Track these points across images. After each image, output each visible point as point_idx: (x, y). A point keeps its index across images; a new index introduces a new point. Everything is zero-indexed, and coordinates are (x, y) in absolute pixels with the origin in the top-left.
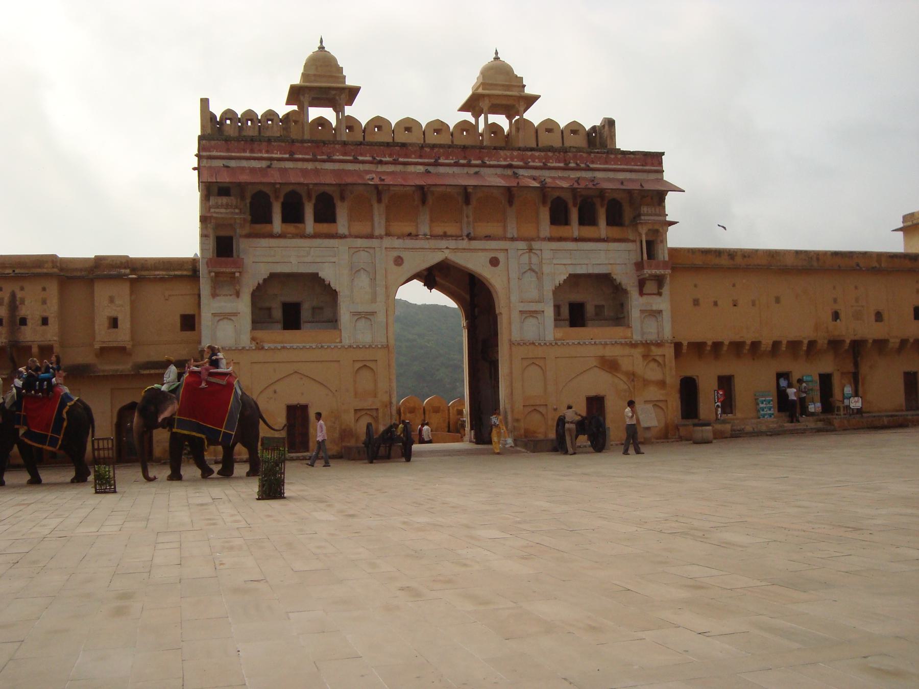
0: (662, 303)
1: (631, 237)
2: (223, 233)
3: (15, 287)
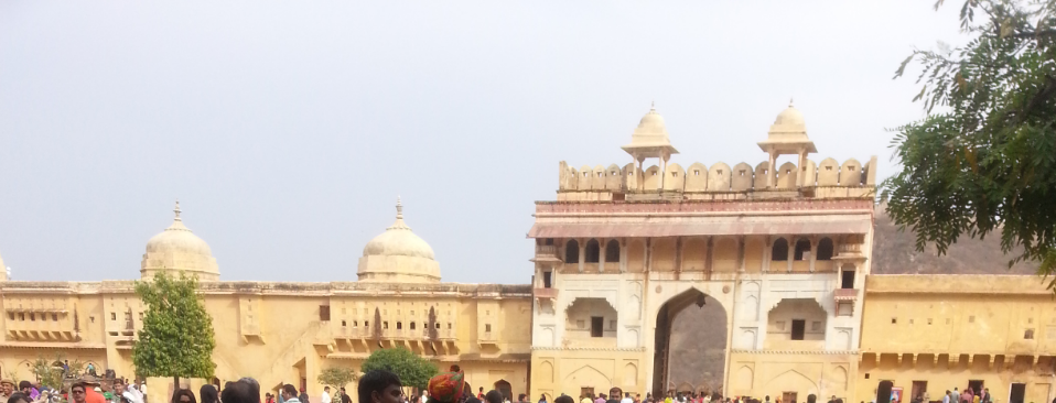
0: (853, 322)
2: (547, 270)
3: (434, 304)
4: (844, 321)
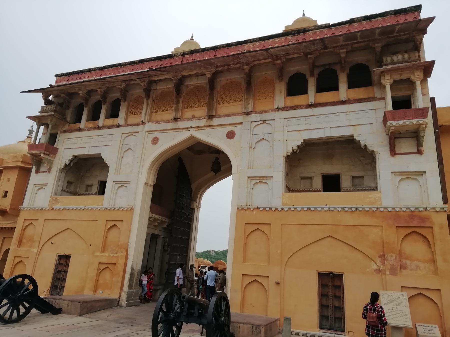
1: (378, 95)
4: (412, 163)
